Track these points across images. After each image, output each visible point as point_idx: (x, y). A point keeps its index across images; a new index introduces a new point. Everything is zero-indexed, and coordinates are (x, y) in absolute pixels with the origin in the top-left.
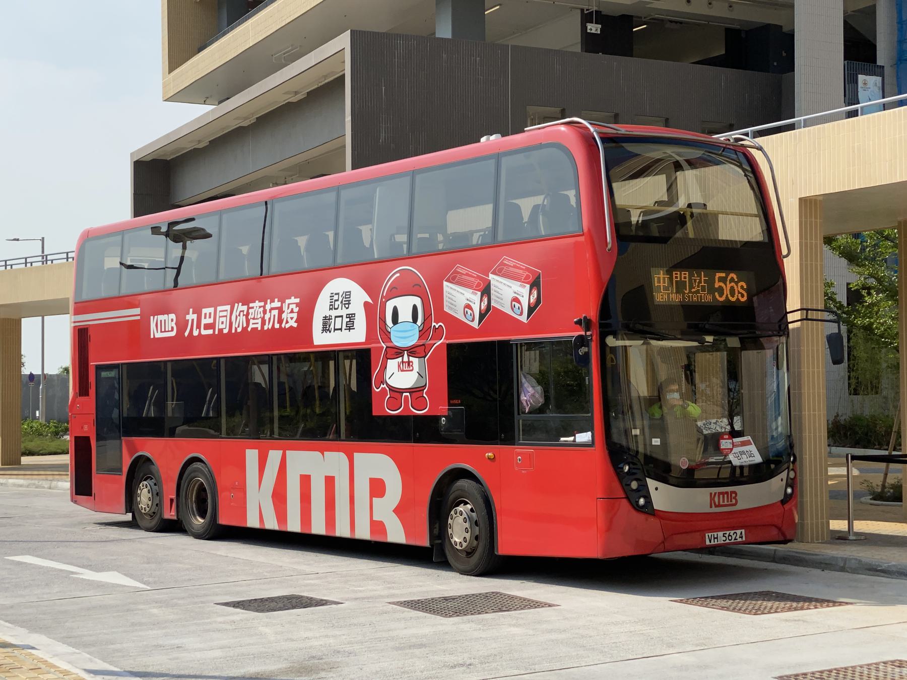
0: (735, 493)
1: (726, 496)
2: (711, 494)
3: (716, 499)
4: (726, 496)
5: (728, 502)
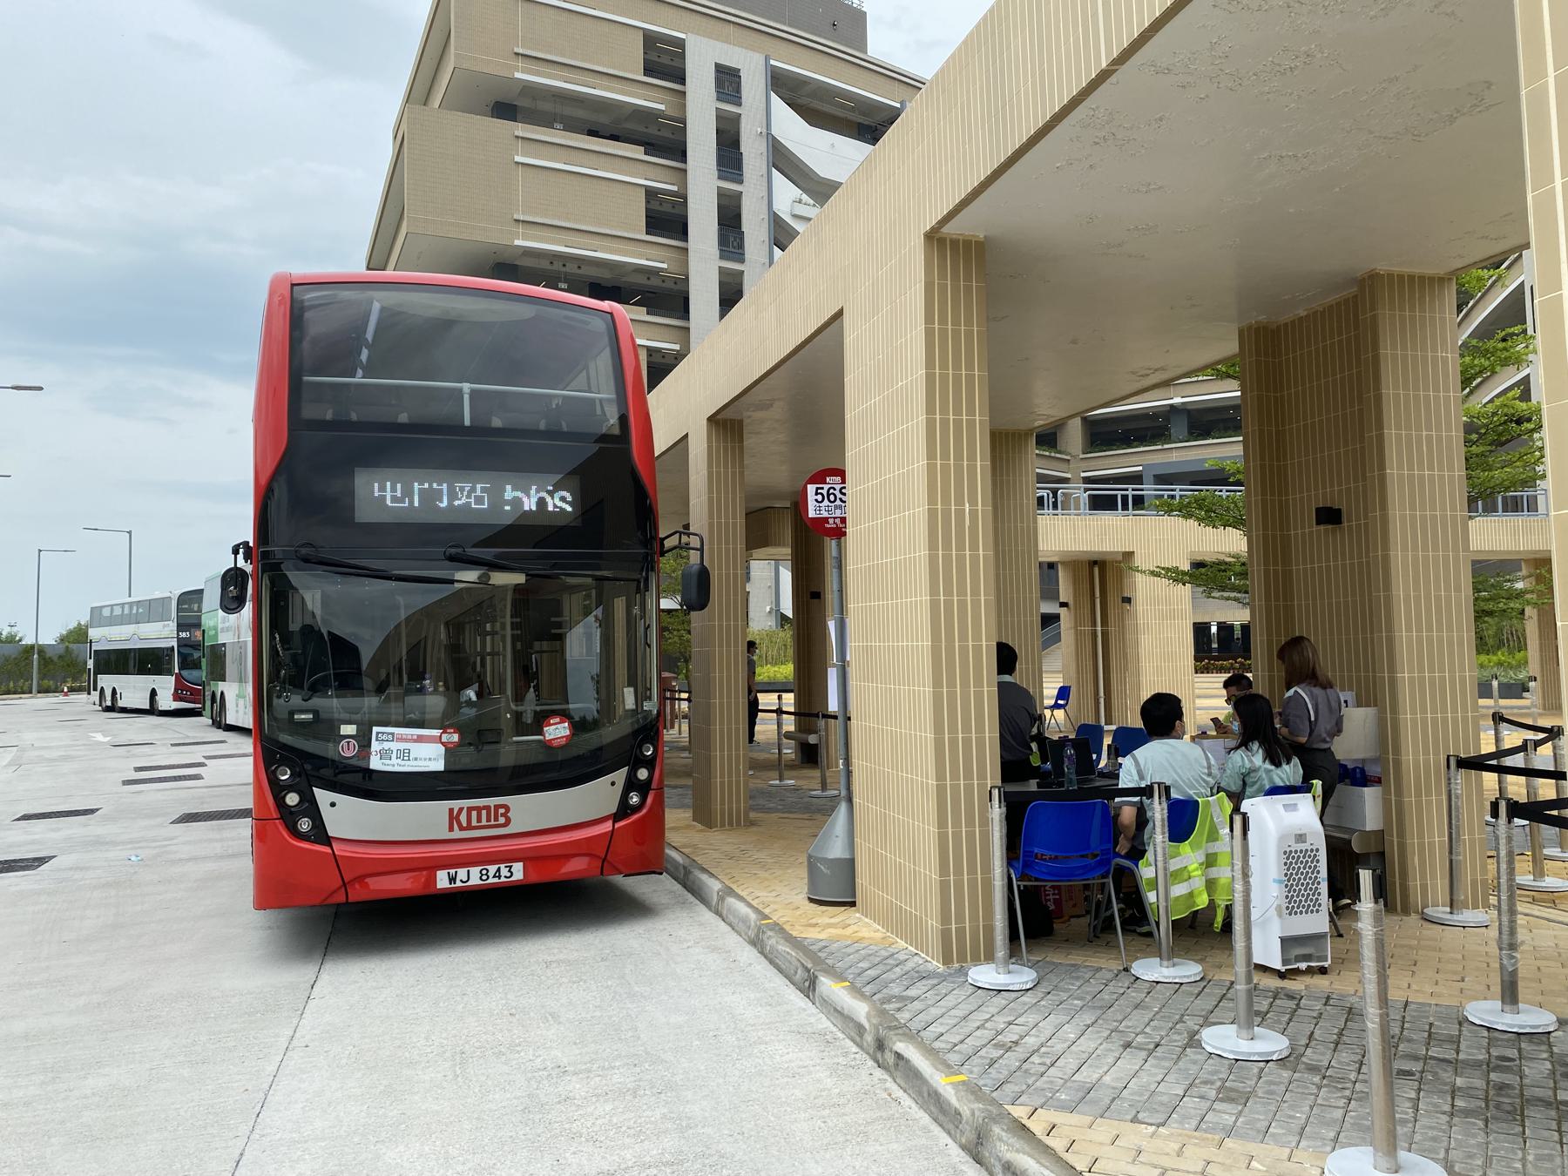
0: (507, 808)
1: (484, 812)
2: (451, 810)
3: (463, 818)
4: (484, 812)
5: (488, 820)
